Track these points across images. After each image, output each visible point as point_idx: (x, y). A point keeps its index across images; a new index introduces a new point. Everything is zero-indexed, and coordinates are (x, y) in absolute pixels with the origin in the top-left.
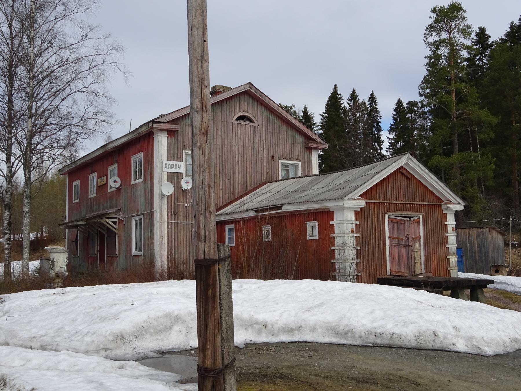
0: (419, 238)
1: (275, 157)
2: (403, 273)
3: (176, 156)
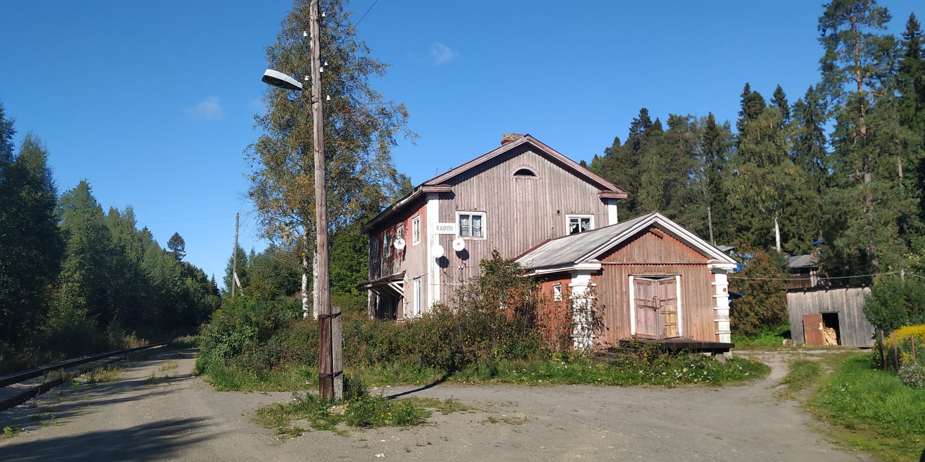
0: (675, 299)
3: (448, 217)
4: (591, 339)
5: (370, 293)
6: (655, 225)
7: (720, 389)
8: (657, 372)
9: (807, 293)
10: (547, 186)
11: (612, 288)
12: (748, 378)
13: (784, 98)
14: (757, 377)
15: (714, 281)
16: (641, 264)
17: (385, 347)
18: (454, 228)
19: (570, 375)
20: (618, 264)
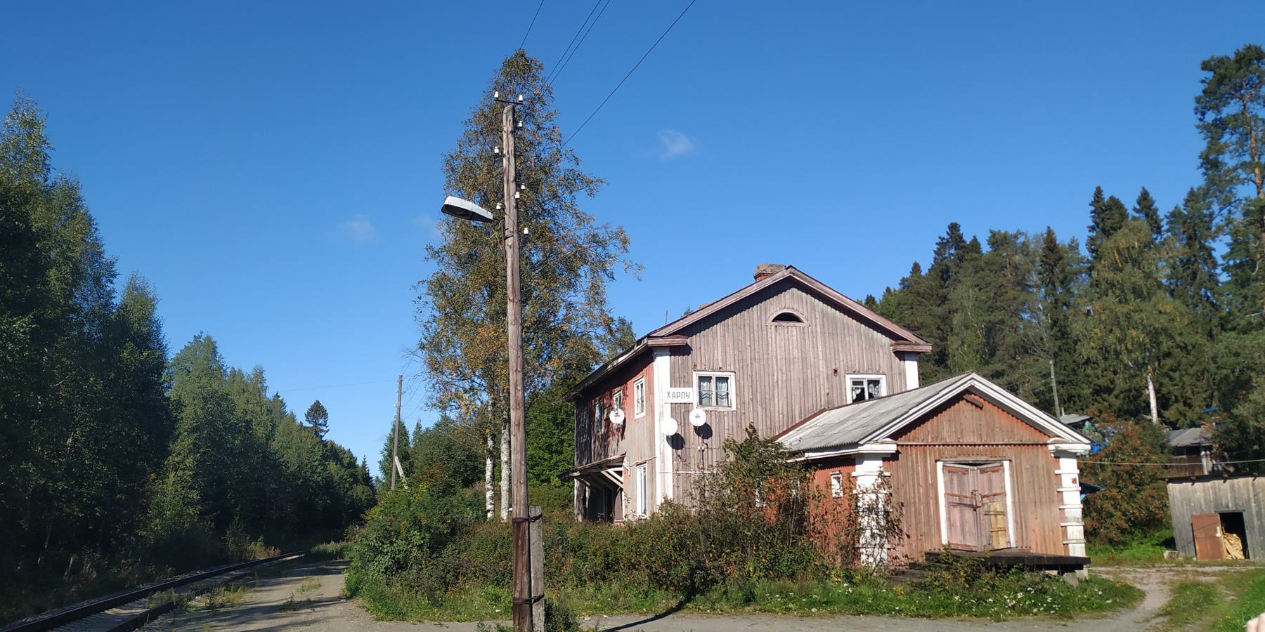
0: (1004, 494)
1: (838, 371)
2: (969, 546)
4: (885, 550)
5: (576, 483)
6: (970, 391)
7: (1070, 623)
8: (980, 599)
9: (1196, 484)
10: (819, 336)
11: (913, 478)
12: (1110, 607)
13: (1152, 205)
14: (1123, 605)
15: (1059, 468)
16: (953, 445)
17: (599, 560)
18: (691, 394)
19: (856, 602)
20: (921, 445)
